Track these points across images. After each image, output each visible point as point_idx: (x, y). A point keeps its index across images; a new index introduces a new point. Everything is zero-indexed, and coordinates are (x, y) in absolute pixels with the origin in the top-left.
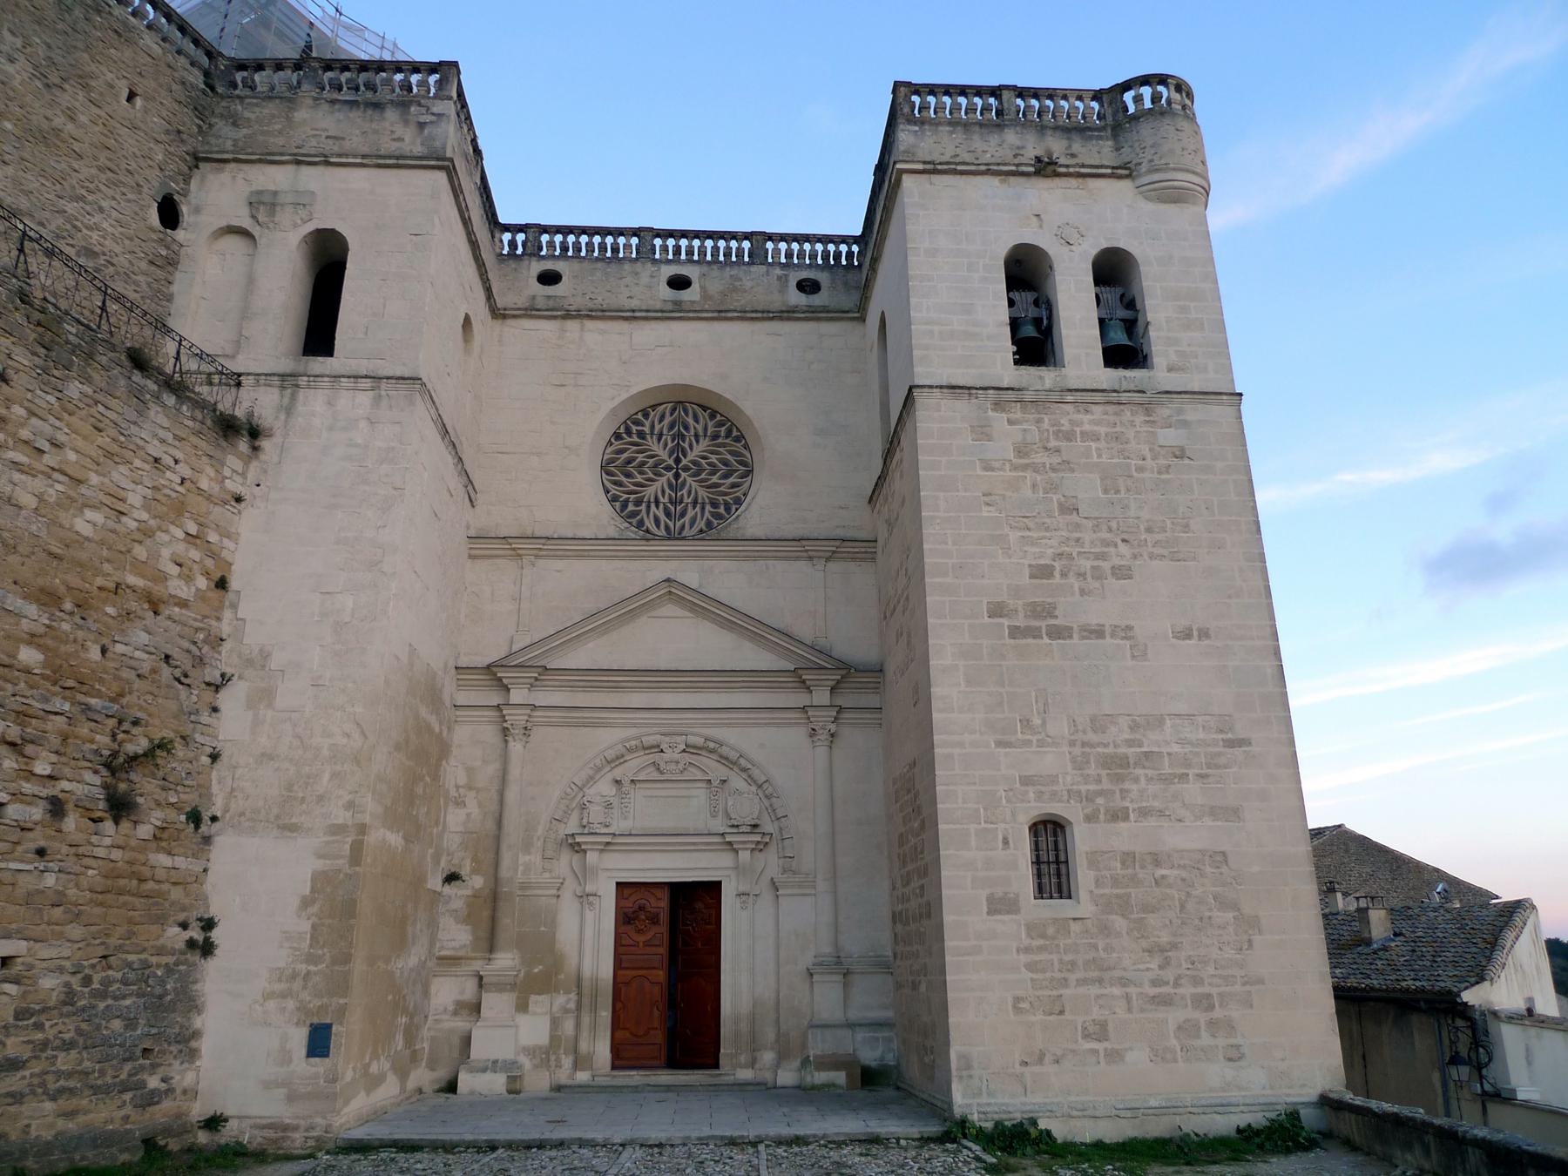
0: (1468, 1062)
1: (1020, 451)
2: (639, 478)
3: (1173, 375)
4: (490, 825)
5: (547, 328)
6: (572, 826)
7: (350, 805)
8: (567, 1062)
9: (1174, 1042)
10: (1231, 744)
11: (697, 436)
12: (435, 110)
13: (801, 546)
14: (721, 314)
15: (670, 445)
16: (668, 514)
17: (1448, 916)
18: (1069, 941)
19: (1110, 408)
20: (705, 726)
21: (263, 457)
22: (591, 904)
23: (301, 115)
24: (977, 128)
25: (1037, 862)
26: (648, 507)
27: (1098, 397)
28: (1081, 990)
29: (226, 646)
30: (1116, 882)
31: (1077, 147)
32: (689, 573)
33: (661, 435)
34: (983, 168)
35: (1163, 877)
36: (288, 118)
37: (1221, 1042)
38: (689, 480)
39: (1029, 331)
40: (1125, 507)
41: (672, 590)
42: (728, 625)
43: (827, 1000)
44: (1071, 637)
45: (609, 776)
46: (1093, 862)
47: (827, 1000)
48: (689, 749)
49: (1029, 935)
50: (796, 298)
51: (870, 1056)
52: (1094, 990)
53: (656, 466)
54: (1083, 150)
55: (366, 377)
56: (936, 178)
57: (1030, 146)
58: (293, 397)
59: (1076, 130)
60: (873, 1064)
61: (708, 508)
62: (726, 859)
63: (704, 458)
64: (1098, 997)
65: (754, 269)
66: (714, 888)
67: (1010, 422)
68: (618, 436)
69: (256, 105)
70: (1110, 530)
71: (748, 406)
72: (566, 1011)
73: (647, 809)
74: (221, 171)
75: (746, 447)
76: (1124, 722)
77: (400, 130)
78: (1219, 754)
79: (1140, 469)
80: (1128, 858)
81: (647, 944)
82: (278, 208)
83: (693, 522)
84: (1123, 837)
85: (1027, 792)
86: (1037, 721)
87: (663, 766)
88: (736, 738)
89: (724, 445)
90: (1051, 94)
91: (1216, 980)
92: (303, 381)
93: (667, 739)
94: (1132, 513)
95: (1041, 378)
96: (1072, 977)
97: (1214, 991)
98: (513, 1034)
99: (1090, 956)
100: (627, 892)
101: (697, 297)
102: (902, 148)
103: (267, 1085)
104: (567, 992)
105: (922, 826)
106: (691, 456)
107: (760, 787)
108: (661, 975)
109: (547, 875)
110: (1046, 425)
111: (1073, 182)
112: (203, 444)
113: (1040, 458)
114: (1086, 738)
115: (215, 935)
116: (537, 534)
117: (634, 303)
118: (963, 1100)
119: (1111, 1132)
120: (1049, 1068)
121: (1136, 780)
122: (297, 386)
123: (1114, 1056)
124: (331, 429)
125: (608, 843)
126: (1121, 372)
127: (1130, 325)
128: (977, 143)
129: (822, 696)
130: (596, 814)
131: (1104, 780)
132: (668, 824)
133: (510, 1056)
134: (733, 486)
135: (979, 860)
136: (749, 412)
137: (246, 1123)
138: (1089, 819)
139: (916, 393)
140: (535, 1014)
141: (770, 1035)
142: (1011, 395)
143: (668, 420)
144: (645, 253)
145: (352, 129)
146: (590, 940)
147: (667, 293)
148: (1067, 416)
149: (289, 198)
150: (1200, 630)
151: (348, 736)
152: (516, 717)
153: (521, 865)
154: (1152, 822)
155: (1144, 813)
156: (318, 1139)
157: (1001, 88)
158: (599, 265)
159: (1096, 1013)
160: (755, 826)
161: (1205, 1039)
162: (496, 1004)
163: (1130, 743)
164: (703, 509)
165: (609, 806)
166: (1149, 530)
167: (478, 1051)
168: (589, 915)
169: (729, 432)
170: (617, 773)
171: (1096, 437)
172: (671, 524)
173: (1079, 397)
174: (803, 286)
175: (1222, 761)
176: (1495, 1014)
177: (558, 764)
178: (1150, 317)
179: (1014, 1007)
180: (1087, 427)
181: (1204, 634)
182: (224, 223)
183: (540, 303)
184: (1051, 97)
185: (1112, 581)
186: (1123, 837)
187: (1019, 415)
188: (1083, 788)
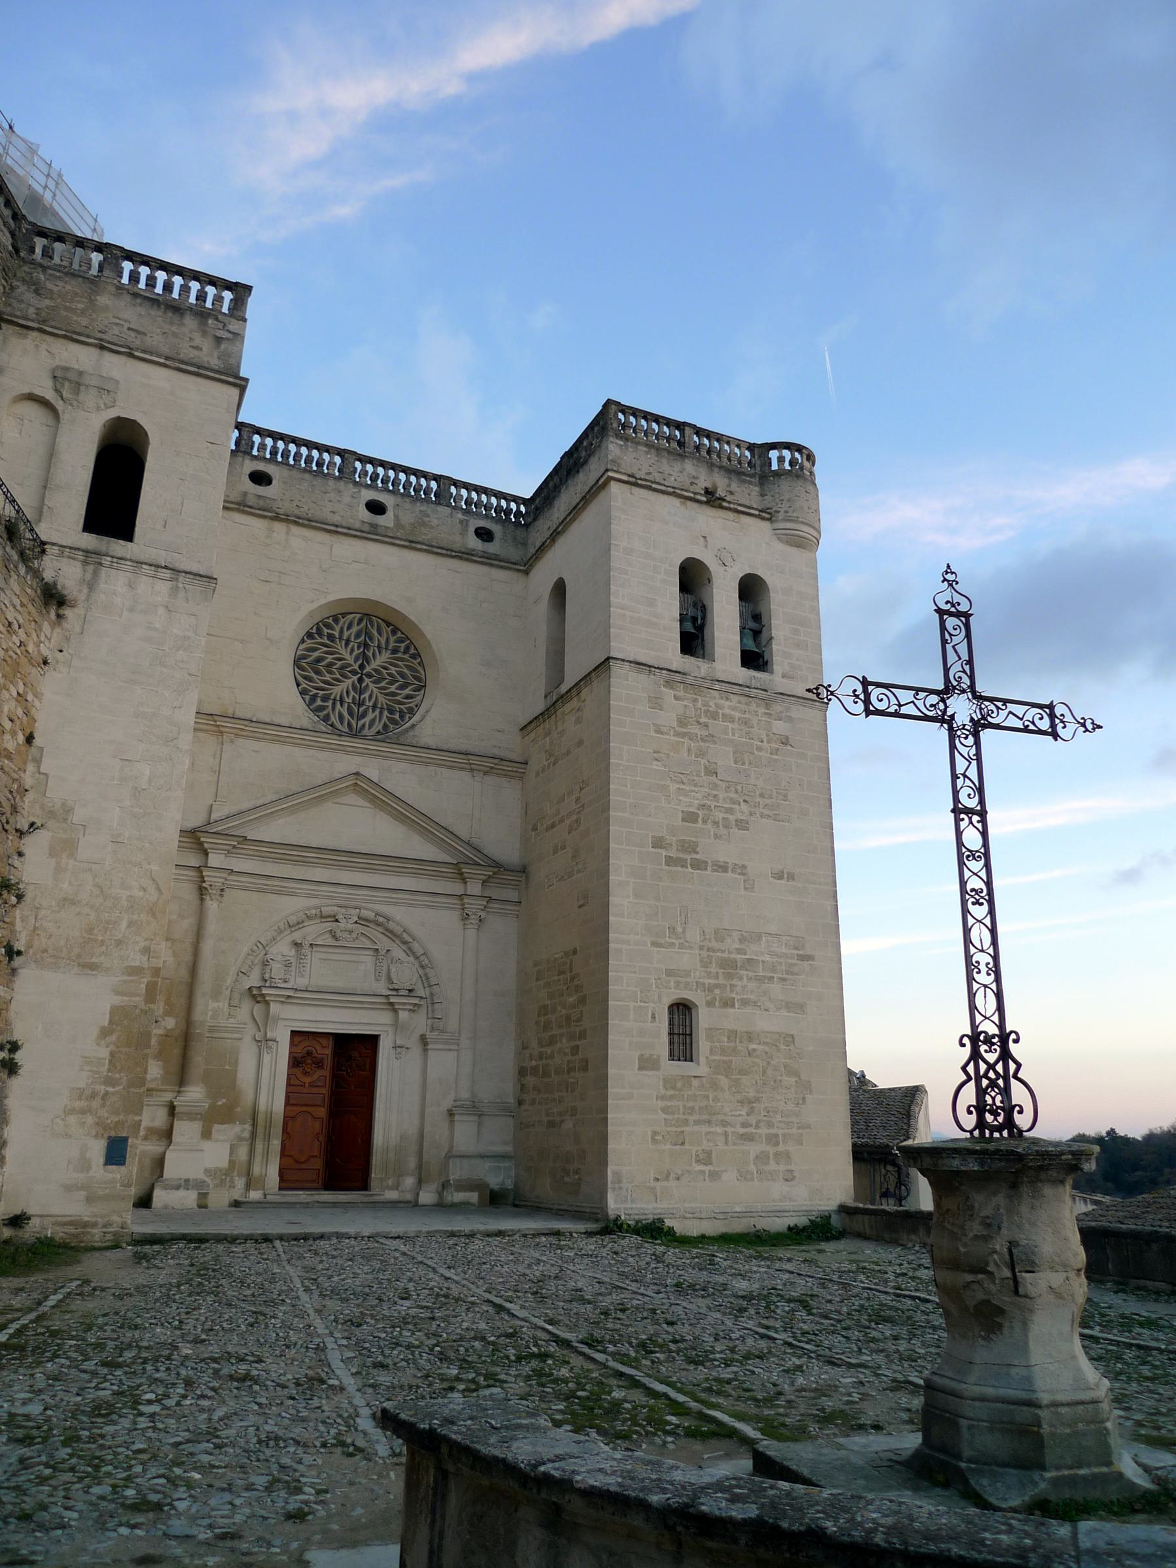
0: (894, 1196)
1: (682, 722)
2: (328, 677)
3: (785, 680)
4: (184, 973)
5: (257, 525)
6: (253, 980)
7: (146, 951)
8: (240, 1183)
9: (753, 1167)
10: (803, 958)
11: (379, 647)
12: (231, 327)
13: (466, 759)
14: (411, 544)
15: (356, 652)
16: (351, 713)
17: (867, 1095)
18: (690, 1093)
19: (743, 699)
20: (375, 902)
21: (65, 625)
22: (270, 1048)
23: (103, 300)
24: (666, 454)
25: (671, 1034)
26: (334, 704)
27: (736, 689)
28: (697, 1128)
29: (29, 797)
30: (723, 1051)
31: (734, 486)
32: (372, 769)
33: (348, 642)
34: (671, 490)
35: (754, 1050)
36: (92, 301)
37: (782, 1168)
38: (371, 685)
39: (690, 628)
40: (748, 776)
41: (359, 784)
42: (402, 818)
43: (465, 1136)
44: (706, 869)
45: (289, 939)
46: (709, 1037)
47: (465, 1136)
48: (362, 921)
50: (474, 543)
51: (495, 1181)
52: (705, 1129)
53: (342, 668)
54: (739, 490)
55: (166, 567)
56: (635, 490)
57: (702, 478)
58: (96, 573)
59: (733, 471)
60: (496, 1188)
61: (386, 713)
62: (385, 1018)
63: (386, 668)
64: (707, 1133)
65: (440, 508)
66: (371, 1041)
67: (676, 698)
68: (309, 635)
69: (59, 278)
70: (737, 792)
71: (428, 629)
72: (241, 1139)
73: (321, 971)
74: (25, 336)
75: (421, 664)
77: (198, 340)
78: (794, 965)
79: (759, 749)
80: (732, 1035)
81: (312, 1085)
82: (82, 388)
84: (731, 1019)
85: (668, 982)
86: (680, 930)
87: (339, 934)
88: (403, 915)
89: (402, 660)
90: (719, 438)
91: (783, 1125)
92: (106, 561)
93: (343, 911)
94: (752, 781)
95: (699, 667)
96: (691, 1118)
97: (780, 1132)
98: (200, 1159)
100: (297, 1039)
101: (391, 525)
102: (610, 457)
103: (68, 1188)
104: (243, 1123)
107: (417, 958)
108: (322, 1112)
109: (232, 1020)
110: (699, 705)
111: (731, 515)
112: (33, 611)
113: (694, 729)
114: (710, 945)
115: (19, 1056)
116: (239, 714)
117: (336, 519)
118: (615, 1205)
119: (712, 1228)
120: (672, 1183)
121: (741, 979)
122: (100, 564)
123: (715, 1176)
124: (131, 610)
125: (289, 997)
127: (756, 634)
128: (665, 466)
129: (474, 888)
130: (277, 970)
131: (721, 976)
132: (339, 983)
133: (201, 1176)
134: (408, 697)
135: (633, 1029)
136: (429, 636)
137: (47, 1221)
138: (710, 1004)
139: (612, 663)
140: (217, 1141)
141: (412, 1163)
142: (678, 677)
143: (355, 629)
144: (345, 473)
145: (156, 329)
146: (265, 1078)
148: (714, 700)
149: (94, 381)
150: (789, 874)
151: (145, 890)
152: (211, 877)
153: (210, 1009)
154: (749, 1010)
155: (745, 1003)
156: (115, 1234)
158: (307, 476)
159: (706, 1145)
160: (410, 991)
161: (772, 1166)
162: (185, 1131)
163: (739, 951)
164: (381, 713)
165: (288, 965)
166: (762, 795)
167: (171, 1171)
168: (267, 1058)
169: (407, 649)
170: (297, 936)
172: (354, 723)
173: (724, 687)
174: (484, 534)
175: (796, 969)
177: (249, 923)
178: (774, 633)
179: (652, 1138)
180: (727, 711)
181: (791, 877)
182: (26, 390)
183: (251, 500)
184: (718, 440)
185: (735, 830)
186: (731, 1019)
187: (681, 694)
188: (707, 981)
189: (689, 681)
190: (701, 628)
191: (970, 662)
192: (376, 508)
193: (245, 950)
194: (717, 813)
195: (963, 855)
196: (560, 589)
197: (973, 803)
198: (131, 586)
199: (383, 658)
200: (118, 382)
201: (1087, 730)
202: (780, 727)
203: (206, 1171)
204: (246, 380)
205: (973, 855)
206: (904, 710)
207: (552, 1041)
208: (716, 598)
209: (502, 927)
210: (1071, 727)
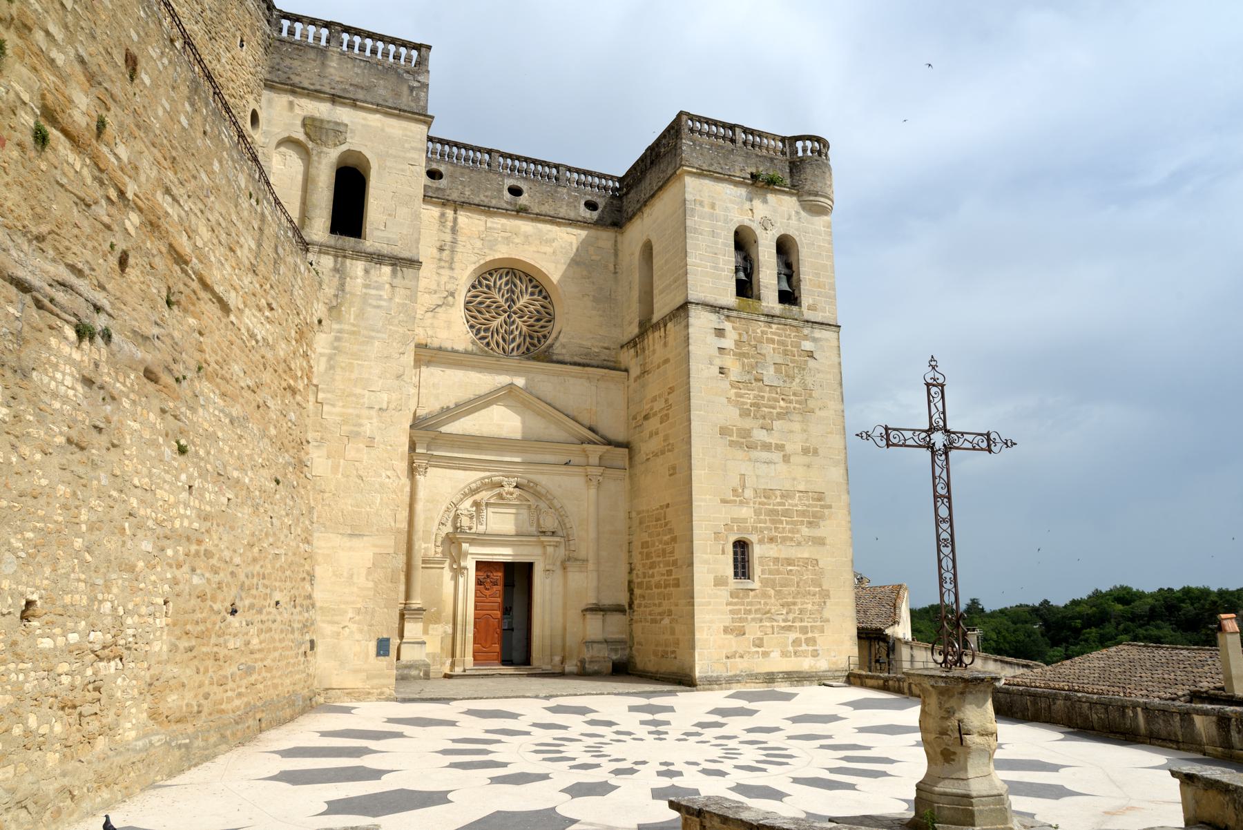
1: (739, 343)
2: (487, 316)
10: (822, 507)
14: (539, 217)
27: (776, 320)
30: (770, 573)
37: (811, 648)
39: (742, 276)
46: (761, 564)
62: (538, 550)
68: (474, 287)
75: (551, 303)
76: (778, 493)
80: (776, 560)
83: (519, 346)
84: (772, 551)
88: (549, 481)
90: (761, 134)
96: (749, 617)
106: (518, 305)
123: (766, 654)
130: (465, 522)
138: (761, 541)
142: (734, 314)
146: (458, 593)
155: (784, 539)
157: (735, 126)
161: (804, 647)
162: (413, 629)
166: (794, 394)
168: (461, 580)
170: (477, 497)
171: (772, 341)
176: (899, 640)
190: (749, 275)
191: (944, 413)
192: (516, 192)
193: (444, 508)
195: (938, 521)
196: (648, 249)
197: (944, 492)
198: (367, 271)
199: (525, 299)
200: (346, 125)
202: (807, 345)
203: (427, 655)
204: (433, 117)
205: (944, 521)
207: (652, 566)
208: (761, 255)
209: (616, 486)
210: (999, 445)
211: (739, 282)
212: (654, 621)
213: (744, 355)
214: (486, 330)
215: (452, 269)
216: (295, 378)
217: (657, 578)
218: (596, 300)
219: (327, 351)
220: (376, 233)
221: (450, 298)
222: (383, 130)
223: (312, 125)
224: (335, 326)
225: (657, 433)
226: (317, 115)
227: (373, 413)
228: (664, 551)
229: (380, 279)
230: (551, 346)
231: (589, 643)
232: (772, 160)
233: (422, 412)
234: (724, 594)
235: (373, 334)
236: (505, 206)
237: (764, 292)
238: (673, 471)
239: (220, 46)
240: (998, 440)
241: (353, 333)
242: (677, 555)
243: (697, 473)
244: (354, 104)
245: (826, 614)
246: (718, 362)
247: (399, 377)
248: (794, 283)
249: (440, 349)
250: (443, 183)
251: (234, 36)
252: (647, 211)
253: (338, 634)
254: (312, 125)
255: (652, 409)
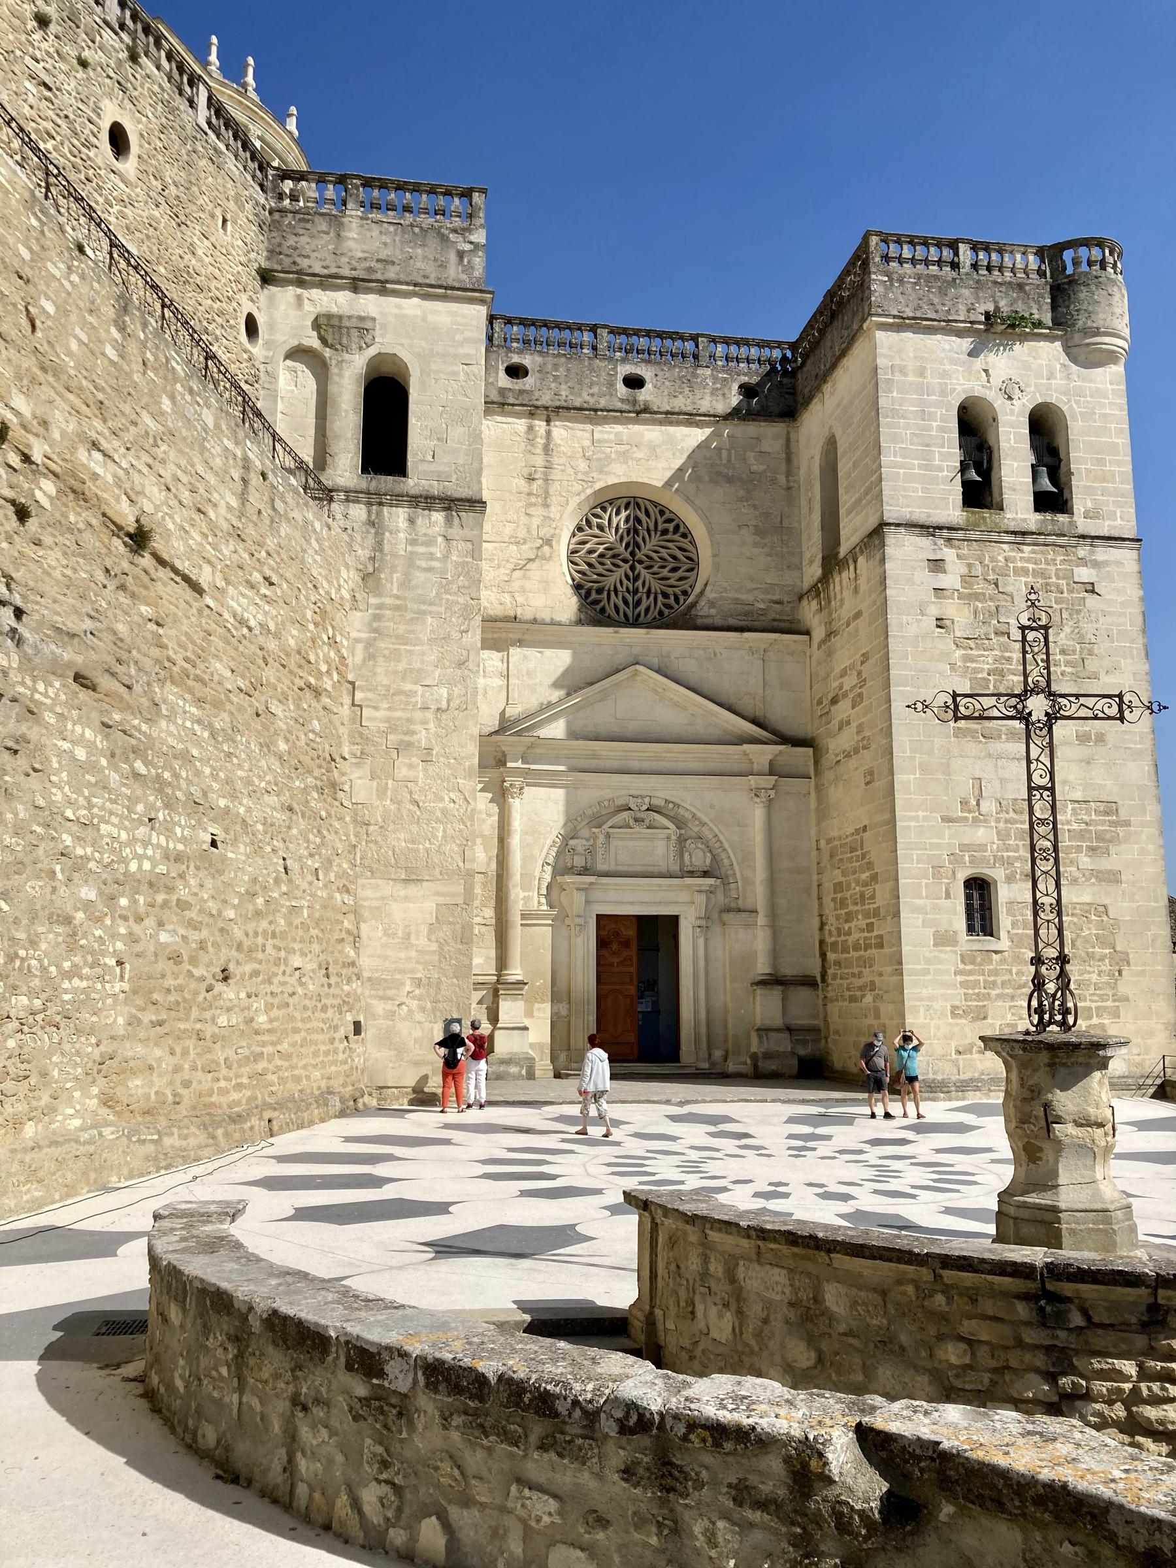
2: (600, 569)
11: (648, 530)
14: (670, 417)
27: (1029, 539)
38: (644, 572)
39: (973, 475)
46: (1010, 912)
49: (963, 962)
61: (660, 598)
66: (674, 920)
68: (580, 529)
75: (693, 542)
83: (647, 610)
96: (994, 993)
97: (1093, 1005)
99: (1006, 978)
105: (874, 878)
126: (1048, 516)
134: (681, 579)
142: (960, 535)
147: (622, 390)
164: (656, 599)
166: (1063, 652)
169: (677, 528)
171: (1025, 572)
180: (1019, 564)
187: (965, 552)
189: (973, 537)
194: (1011, 677)
197: (1045, 781)
198: (412, 521)
200: (374, 319)
201: (1153, 712)
202: (1084, 574)
203: (532, 1046)
205: (1043, 822)
206: (986, 714)
207: (849, 918)
208: (1002, 438)
211: (965, 484)
212: (853, 999)
213: (976, 596)
214: (600, 591)
215: (546, 506)
216: (319, 675)
217: (855, 936)
218: (759, 531)
219: (364, 635)
220: (423, 467)
221: (546, 548)
222: (424, 319)
223: (325, 325)
224: (373, 601)
225: (848, 723)
226: (334, 310)
227: (430, 715)
228: (862, 895)
229: (430, 532)
230: (693, 605)
231: (763, 1031)
232: (1020, 287)
233: (512, 712)
234: (949, 958)
235: (424, 607)
236: (619, 405)
237: (1008, 497)
238: (870, 777)
239: (193, 234)
240: (1136, 702)
241: (397, 608)
242: (879, 902)
243: (905, 779)
244: (383, 288)
245: (1123, 988)
246: (934, 611)
247: (461, 664)
248: (1063, 479)
249: (535, 621)
250: (529, 382)
251: (213, 216)
252: (827, 388)
253: (393, 1013)
254: (325, 325)
255: (841, 688)
